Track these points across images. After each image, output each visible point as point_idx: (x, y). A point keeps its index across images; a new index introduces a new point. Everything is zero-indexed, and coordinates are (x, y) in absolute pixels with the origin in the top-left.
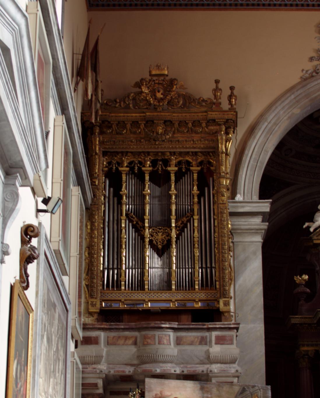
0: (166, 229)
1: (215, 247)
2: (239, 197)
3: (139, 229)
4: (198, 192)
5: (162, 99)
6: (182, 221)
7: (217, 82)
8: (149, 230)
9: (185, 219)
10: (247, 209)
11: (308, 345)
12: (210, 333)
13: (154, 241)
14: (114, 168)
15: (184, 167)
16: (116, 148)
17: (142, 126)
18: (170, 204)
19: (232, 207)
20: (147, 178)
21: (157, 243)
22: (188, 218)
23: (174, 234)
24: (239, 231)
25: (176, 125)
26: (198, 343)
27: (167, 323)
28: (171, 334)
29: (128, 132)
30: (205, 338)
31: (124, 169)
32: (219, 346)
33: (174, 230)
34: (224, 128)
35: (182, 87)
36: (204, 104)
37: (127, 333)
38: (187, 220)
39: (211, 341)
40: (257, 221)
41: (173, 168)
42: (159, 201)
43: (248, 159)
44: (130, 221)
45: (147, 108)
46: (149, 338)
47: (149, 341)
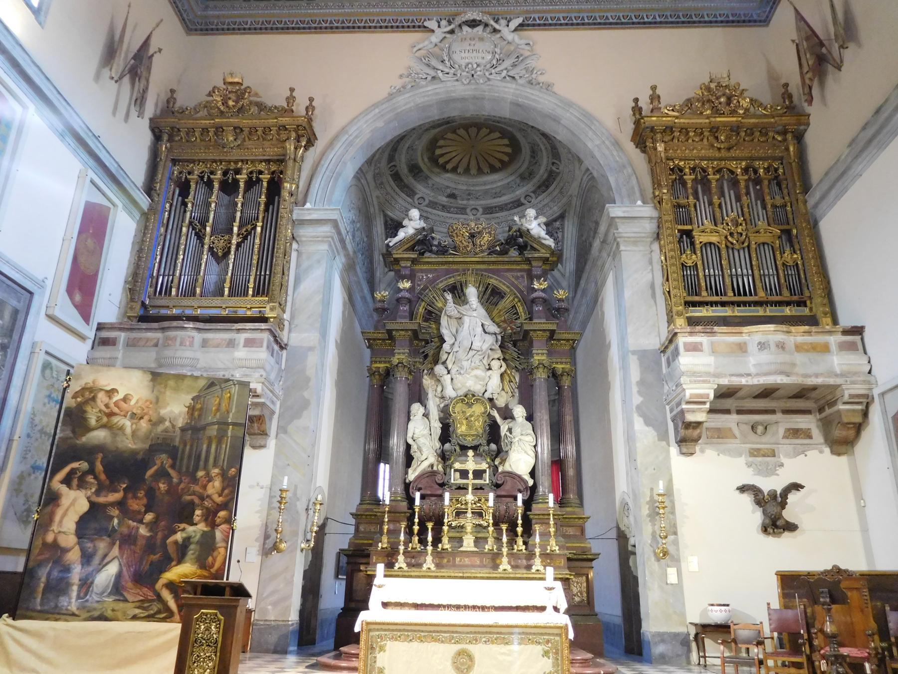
2: (308, 205)
3: (200, 237)
5: (233, 106)
7: (292, 90)
9: (249, 227)
10: (314, 216)
11: (380, 362)
12: (239, 335)
15: (255, 175)
18: (235, 211)
19: (297, 214)
20: (216, 185)
23: (234, 241)
28: (198, 337)
29: (198, 140)
31: (194, 177)
33: (235, 237)
34: (293, 135)
35: (256, 95)
36: (276, 111)
37: (149, 335)
39: (238, 345)
40: (326, 230)
41: (242, 178)
43: (324, 170)
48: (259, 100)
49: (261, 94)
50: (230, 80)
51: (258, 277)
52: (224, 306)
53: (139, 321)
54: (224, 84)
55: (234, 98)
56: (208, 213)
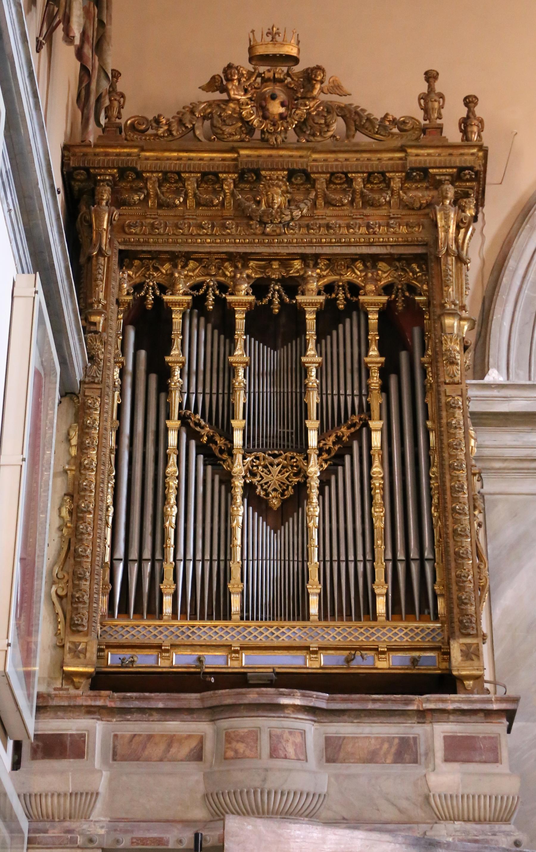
0: (293, 458)
1: (430, 505)
4: (383, 359)
5: (282, 117)
6: (337, 436)
8: (244, 458)
9: (344, 431)
12: (427, 727)
13: (259, 488)
14: (151, 298)
15: (341, 296)
16: (155, 243)
17: (229, 186)
18: (304, 389)
21: (267, 494)
22: (353, 430)
24: (497, 465)
25: (321, 184)
26: (390, 758)
27: (298, 692)
29: (191, 202)
30: (412, 742)
32: (456, 766)
33: (313, 458)
38: (352, 434)
39: (430, 751)
42: (273, 384)
43: (517, 282)
44: (193, 434)
45: (242, 141)
46: (242, 739)
47: (241, 747)
48: (344, 101)
49: (346, 86)
50: (261, 50)
51: (401, 567)
52: (314, 647)
53: (93, 687)
54: (251, 60)
55: (282, 97)
56: (231, 390)
